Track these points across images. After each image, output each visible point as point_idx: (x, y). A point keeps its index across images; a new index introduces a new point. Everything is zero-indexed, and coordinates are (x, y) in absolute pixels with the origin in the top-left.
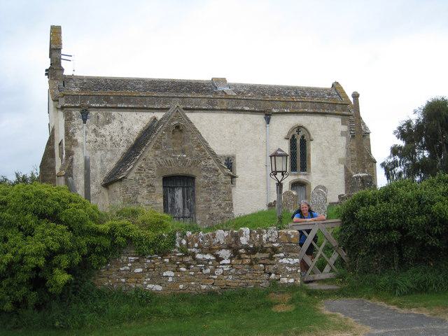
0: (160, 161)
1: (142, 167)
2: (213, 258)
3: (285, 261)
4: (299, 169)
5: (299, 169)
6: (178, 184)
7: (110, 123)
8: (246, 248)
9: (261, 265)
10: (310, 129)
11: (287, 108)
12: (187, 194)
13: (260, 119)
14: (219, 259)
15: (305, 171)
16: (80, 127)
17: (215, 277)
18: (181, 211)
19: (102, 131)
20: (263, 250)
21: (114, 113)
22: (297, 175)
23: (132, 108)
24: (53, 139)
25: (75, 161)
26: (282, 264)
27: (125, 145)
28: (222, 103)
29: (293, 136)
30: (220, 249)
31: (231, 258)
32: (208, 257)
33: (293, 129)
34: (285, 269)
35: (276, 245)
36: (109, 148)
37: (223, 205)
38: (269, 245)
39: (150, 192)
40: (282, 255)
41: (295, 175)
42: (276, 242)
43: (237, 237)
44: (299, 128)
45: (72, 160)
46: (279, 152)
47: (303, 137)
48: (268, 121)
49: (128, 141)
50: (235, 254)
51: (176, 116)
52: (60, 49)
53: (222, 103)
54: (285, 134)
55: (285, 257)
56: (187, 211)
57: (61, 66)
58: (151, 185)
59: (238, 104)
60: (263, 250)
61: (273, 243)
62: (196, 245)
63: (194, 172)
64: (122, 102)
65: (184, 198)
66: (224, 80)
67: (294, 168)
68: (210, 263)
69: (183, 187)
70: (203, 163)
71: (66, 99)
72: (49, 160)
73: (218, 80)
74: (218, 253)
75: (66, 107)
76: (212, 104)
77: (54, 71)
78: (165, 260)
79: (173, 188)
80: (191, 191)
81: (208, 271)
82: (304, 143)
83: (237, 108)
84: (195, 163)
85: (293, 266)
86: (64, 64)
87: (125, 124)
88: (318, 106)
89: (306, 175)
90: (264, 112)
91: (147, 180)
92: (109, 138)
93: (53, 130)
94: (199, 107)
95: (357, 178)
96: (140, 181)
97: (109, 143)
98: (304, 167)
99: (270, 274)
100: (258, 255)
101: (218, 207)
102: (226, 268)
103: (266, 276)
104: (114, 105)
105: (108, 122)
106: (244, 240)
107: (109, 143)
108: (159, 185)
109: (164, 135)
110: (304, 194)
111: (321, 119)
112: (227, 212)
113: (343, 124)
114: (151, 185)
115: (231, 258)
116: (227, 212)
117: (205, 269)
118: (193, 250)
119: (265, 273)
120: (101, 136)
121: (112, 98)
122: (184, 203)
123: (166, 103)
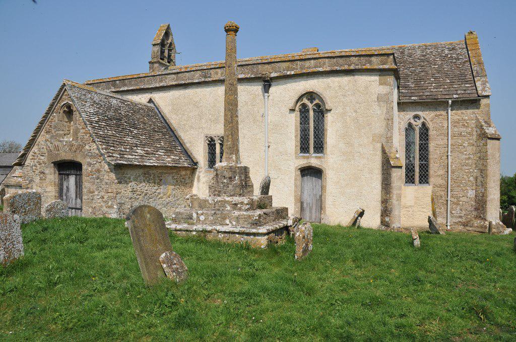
4: (312, 149)
5: (312, 149)
6: (72, 172)
13: (258, 88)
15: (322, 152)
18: (74, 201)
23: (132, 90)
28: (217, 73)
33: (300, 98)
37: (106, 197)
41: (304, 157)
44: (311, 95)
48: (266, 89)
53: (217, 73)
54: (291, 105)
56: (79, 200)
58: (42, 173)
63: (79, 159)
64: (125, 85)
65: (77, 187)
67: (304, 148)
69: (76, 175)
70: (87, 147)
76: (205, 77)
79: (68, 175)
88: (341, 61)
89: (320, 157)
91: (38, 166)
96: (34, 167)
98: (320, 147)
101: (101, 200)
110: (320, 184)
111: (345, 80)
113: (381, 84)
114: (42, 173)
121: (118, 82)
123: (161, 81)
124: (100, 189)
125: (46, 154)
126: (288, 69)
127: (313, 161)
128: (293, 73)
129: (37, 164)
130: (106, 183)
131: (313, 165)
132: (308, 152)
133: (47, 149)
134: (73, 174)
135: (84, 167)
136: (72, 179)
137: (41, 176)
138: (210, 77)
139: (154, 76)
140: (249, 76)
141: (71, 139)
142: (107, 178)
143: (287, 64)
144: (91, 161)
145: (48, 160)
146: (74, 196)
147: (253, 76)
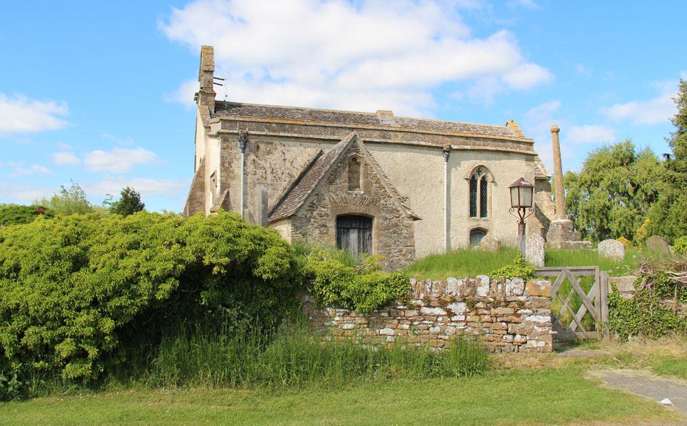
0: (335, 197)
1: (314, 204)
2: (445, 313)
3: (533, 318)
6: (354, 225)
7: (271, 153)
8: (483, 300)
9: (504, 324)
10: (492, 169)
11: (468, 144)
12: (364, 237)
14: (450, 314)
16: (237, 156)
17: (447, 337)
19: (262, 163)
20: (507, 303)
21: (275, 142)
22: (478, 220)
24: (204, 170)
25: (231, 194)
26: (529, 323)
27: (288, 179)
29: (473, 177)
30: (454, 301)
31: (465, 314)
32: (438, 311)
34: (533, 329)
35: (522, 299)
36: (269, 181)
37: (404, 251)
38: (513, 298)
39: (321, 233)
40: (527, 311)
42: (522, 295)
43: (473, 287)
44: (479, 169)
45: (228, 192)
46: (523, 183)
47: (484, 178)
49: (291, 176)
50: (472, 305)
51: (353, 147)
52: (212, 72)
53: (397, 136)
55: (535, 313)
57: (212, 90)
58: (324, 226)
59: (414, 139)
60: (507, 303)
61: (519, 296)
62: (422, 296)
63: (372, 213)
64: (284, 131)
65: (359, 242)
66: (390, 113)
68: (440, 319)
69: (359, 229)
70: (382, 202)
71: (223, 125)
72: (199, 194)
73: (383, 113)
74: (450, 306)
75: (223, 133)
76: (384, 138)
77: (206, 93)
78: (383, 314)
79: (348, 229)
80: (368, 233)
81: (437, 329)
82: (484, 182)
83: (412, 142)
84: (374, 202)
85: (544, 325)
86: (216, 88)
87: (288, 156)
89: (486, 220)
90: (442, 148)
91: (319, 218)
92: (269, 171)
93: (203, 161)
94: (371, 140)
95: (557, 224)
97: (270, 177)
98: (483, 213)
99: (514, 335)
100: (499, 310)
102: (461, 326)
103: (510, 337)
104: (277, 134)
105: (269, 153)
106: (482, 291)
107: (270, 177)
108: (332, 225)
109: (339, 167)
112: (407, 260)
115: (465, 314)
116: (407, 260)
117: (434, 326)
118: (419, 302)
119: (508, 333)
120: (261, 168)
121: (274, 125)
122: (359, 248)
123: (334, 134)
124: (398, 243)
125: (329, 206)
126: (464, 144)
127: (483, 224)
128: (469, 147)
129: (317, 217)
130: (405, 237)
131: (482, 227)
132: (475, 216)
133: (330, 201)
134: (354, 228)
135: (375, 222)
136: (353, 236)
137: (323, 229)
138: (389, 138)
139: (325, 126)
140: (430, 144)
141: (362, 192)
142: (406, 231)
143: (463, 140)
144: (388, 216)
145: (332, 211)
146: (357, 250)
147: (434, 145)
